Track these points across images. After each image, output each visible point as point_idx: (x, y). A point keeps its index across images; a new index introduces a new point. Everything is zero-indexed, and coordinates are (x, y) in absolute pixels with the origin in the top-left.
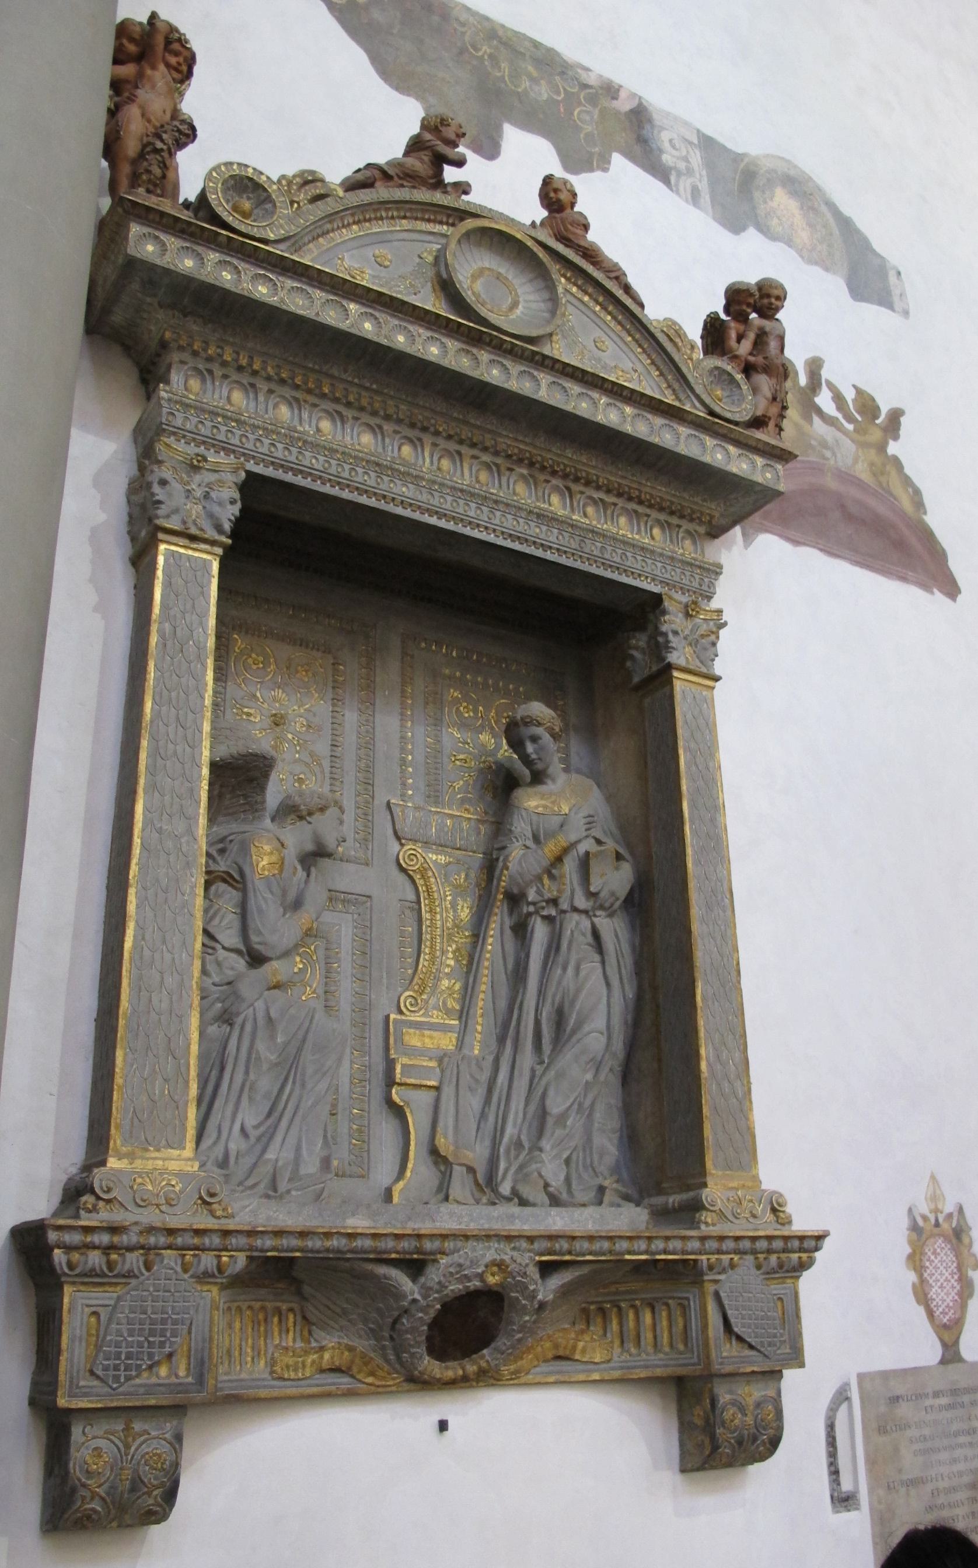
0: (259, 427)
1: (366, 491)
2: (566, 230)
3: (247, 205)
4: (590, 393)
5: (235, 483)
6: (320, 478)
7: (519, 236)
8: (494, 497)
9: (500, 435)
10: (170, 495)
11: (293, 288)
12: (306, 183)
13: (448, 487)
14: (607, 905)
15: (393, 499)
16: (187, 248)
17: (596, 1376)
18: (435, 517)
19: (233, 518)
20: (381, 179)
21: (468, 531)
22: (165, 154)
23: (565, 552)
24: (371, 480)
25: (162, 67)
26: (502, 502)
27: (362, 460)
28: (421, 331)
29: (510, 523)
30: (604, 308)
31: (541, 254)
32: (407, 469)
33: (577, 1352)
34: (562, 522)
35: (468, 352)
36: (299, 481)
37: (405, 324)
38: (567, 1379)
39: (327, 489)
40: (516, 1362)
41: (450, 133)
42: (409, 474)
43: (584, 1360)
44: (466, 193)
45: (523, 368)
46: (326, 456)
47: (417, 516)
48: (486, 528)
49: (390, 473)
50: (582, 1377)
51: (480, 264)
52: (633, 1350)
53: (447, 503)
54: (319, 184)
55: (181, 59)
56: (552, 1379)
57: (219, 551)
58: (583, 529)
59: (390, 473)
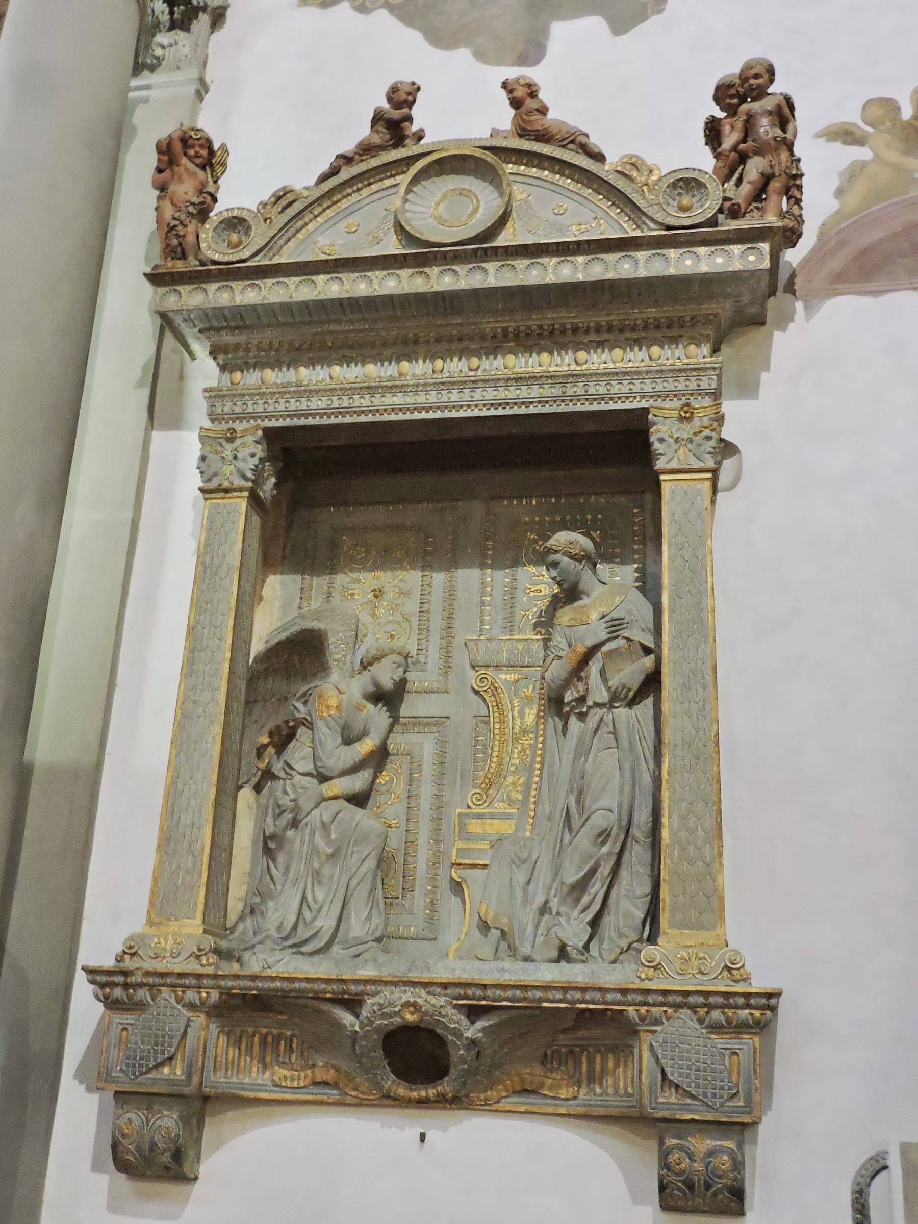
0: (274, 393)
1: (363, 412)
2: (523, 121)
3: (234, 237)
4: (538, 260)
5: (257, 442)
6: (325, 414)
7: (468, 152)
8: (472, 379)
9: (482, 323)
10: (209, 466)
11: (273, 284)
12: (280, 198)
13: (430, 385)
14: (622, 696)
15: (385, 410)
16: (196, 288)
17: (563, 1111)
18: (424, 412)
19: (253, 467)
20: (345, 164)
21: (454, 414)
22: (180, 227)
23: (547, 402)
24: (366, 402)
25: (184, 161)
26: (480, 380)
27: (357, 388)
28: (378, 273)
29: (490, 394)
30: (563, 175)
31: (490, 157)
32: (392, 383)
33: (546, 1087)
34: (541, 377)
35: (421, 273)
36: (311, 421)
37: (365, 274)
38: (536, 1109)
39: (333, 420)
40: (486, 1091)
41: (402, 96)
42: (396, 386)
43: (551, 1095)
44: (420, 138)
45: (471, 266)
46: (328, 396)
47: (408, 416)
48: (469, 406)
49: (380, 391)
50: (550, 1110)
51: (444, 190)
52: (598, 1090)
53: (433, 397)
54: (288, 195)
55: (197, 149)
56: (522, 1109)
57: (246, 494)
58: (563, 377)
59: (380, 391)
